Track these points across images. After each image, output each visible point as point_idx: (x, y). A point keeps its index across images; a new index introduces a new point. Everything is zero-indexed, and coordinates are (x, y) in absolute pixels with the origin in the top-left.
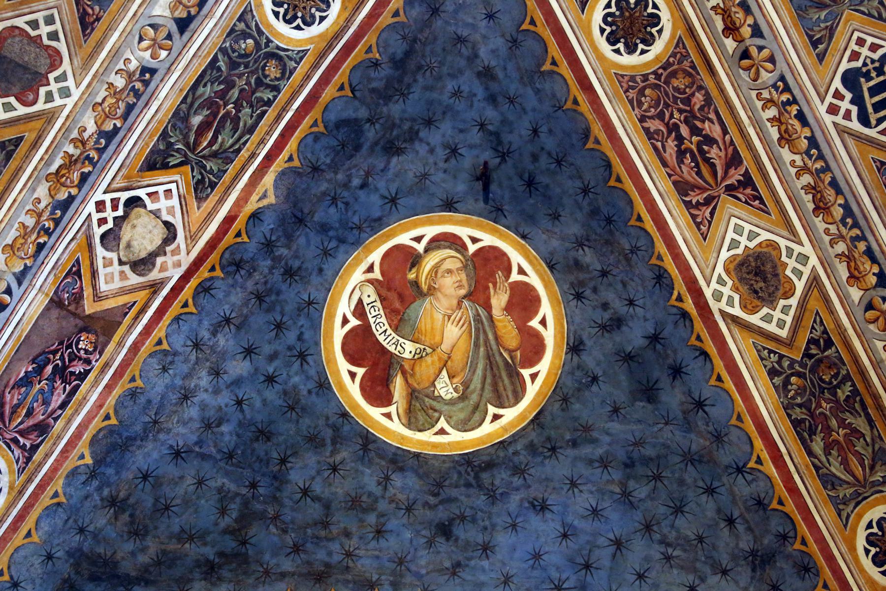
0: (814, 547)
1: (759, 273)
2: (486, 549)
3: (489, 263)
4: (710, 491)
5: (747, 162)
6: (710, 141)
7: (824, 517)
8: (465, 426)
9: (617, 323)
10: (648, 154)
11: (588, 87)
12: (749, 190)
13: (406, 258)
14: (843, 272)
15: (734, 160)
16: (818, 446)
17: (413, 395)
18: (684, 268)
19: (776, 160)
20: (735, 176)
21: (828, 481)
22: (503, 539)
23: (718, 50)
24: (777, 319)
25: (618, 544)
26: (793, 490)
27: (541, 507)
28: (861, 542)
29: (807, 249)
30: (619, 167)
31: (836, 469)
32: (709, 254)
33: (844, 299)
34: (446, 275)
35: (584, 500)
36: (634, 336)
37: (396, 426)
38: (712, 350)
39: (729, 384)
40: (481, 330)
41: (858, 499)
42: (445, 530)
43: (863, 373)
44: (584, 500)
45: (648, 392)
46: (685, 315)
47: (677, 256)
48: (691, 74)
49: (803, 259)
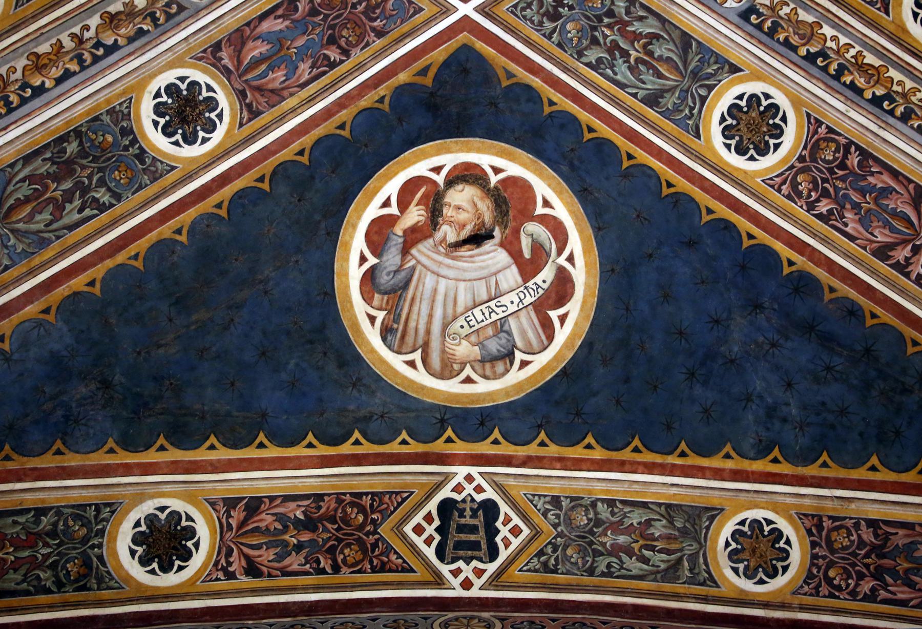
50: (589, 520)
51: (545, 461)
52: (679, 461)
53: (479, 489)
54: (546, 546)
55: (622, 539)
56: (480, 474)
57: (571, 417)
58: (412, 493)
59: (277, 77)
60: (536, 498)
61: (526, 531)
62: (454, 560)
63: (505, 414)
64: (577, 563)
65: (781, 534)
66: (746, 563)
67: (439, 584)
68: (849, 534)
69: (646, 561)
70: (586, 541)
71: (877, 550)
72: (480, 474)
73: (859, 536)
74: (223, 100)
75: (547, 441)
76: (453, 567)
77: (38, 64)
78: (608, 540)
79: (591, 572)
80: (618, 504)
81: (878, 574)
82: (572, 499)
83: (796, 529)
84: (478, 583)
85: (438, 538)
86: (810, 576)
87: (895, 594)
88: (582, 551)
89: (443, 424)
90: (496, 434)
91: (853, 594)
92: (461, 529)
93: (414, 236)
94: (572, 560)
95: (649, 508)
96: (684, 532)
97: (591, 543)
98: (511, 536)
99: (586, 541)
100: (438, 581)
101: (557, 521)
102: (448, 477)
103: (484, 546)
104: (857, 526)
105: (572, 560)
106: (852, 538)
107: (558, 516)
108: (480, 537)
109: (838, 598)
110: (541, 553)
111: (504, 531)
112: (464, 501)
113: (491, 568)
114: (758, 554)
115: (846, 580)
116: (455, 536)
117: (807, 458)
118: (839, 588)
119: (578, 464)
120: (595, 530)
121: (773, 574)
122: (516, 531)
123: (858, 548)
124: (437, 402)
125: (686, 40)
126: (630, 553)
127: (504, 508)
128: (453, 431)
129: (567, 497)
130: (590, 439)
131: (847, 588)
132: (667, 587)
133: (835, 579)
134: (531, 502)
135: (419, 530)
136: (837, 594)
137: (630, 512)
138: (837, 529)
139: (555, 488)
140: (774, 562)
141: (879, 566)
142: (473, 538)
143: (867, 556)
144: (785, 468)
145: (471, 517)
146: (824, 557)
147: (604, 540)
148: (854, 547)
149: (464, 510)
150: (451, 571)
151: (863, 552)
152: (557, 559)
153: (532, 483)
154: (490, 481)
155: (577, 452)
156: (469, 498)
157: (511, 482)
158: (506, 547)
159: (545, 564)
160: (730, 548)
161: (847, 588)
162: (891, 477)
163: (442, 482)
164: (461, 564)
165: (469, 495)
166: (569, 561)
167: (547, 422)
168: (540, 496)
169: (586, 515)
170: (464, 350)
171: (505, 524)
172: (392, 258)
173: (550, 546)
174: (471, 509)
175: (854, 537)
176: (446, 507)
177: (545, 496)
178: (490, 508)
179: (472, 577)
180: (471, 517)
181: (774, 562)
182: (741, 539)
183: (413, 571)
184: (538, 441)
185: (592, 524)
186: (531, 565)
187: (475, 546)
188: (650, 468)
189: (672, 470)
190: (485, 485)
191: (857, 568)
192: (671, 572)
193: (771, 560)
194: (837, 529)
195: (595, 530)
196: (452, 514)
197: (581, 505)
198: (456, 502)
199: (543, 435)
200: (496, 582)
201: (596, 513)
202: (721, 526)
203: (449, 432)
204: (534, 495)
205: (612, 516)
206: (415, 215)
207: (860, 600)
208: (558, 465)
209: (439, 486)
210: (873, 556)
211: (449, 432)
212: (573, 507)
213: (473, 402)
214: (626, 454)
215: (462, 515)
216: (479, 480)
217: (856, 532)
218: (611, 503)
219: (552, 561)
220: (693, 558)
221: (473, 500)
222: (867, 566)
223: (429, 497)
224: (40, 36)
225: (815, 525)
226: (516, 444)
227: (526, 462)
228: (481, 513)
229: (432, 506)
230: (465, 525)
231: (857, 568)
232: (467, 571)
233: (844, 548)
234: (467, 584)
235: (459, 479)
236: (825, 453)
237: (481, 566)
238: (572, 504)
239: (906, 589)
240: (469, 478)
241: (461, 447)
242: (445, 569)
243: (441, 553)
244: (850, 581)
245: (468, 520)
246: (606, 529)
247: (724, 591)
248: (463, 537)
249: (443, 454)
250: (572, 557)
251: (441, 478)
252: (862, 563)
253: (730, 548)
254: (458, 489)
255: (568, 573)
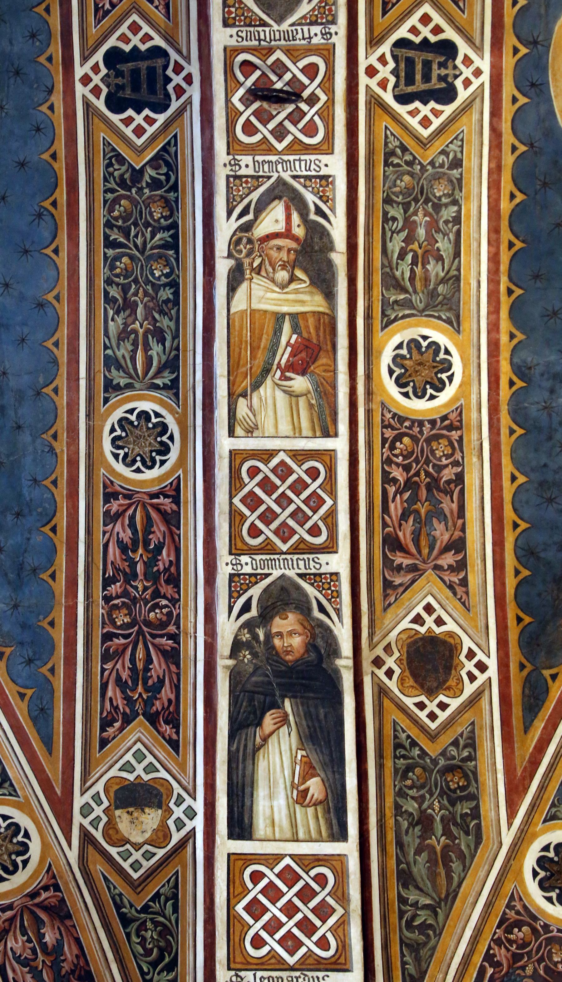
50: (440, 198)
51: (497, 151)
52: (503, 288)
53: (467, 83)
54: (411, 154)
55: (421, 232)
56: (482, 84)
57: (542, 178)
58: (464, 12)
60: (460, 143)
61: (426, 133)
62: (395, 58)
63: (543, 109)
64: (395, 186)
65: (440, 390)
66: (408, 356)
67: (371, 42)
68: (447, 457)
69: (402, 256)
70: (418, 195)
71: (434, 484)
72: (482, 84)
73: (446, 466)
75: (517, 153)
76: (389, 57)
78: (420, 218)
79: (388, 201)
80: (456, 227)
81: (410, 484)
82: (460, 180)
83: (446, 405)
84: (373, 83)
85: (417, 40)
86: (402, 420)
87: (393, 502)
88: (407, 192)
89: (533, 43)
90: (523, 100)
91: (388, 461)
92: (427, 65)
94: (398, 182)
95: (454, 259)
96: (433, 294)
97: (416, 200)
98: (419, 117)
99: (418, 195)
100: (374, 42)
101: (437, 165)
102: (479, 50)
103: (410, 89)
104: (456, 464)
105: (398, 182)
106: (443, 459)
107: (442, 166)
108: (420, 86)
109: (383, 447)
110: (404, 149)
111: (425, 110)
112: (455, 67)
113: (388, 97)
114: (418, 368)
115: (401, 454)
116: (419, 58)
117: (518, 413)
118: (392, 447)
119: (495, 186)
120: (430, 204)
121: (400, 383)
122: (426, 122)
123: (434, 466)
124: (554, 36)
126: (408, 240)
127: (448, 110)
128: (525, 55)
129: (461, 174)
130: (520, 197)
131: (393, 455)
132: (377, 278)
133: (401, 443)
134: (456, 138)
135: (426, 19)
136: (387, 445)
137: (449, 239)
138: (451, 444)
139: (470, 162)
140: (412, 384)
141: (419, 486)
142: (418, 77)
143: (428, 474)
144: (505, 393)
145: (439, 75)
146: (421, 432)
147: (420, 213)
148: (435, 461)
149: (446, 68)
150: (383, 55)
151: (431, 470)
152: (398, 165)
153: (475, 138)
154: (475, 94)
155: (507, 184)
156: (458, 73)
157: (475, 117)
158: (410, 113)
159: (393, 153)
160: (421, 340)
161: (393, 455)
162: (508, 496)
163: (474, 44)
164: (392, 65)
165: (461, 73)
166: (397, 178)
167: (536, 153)
168: (462, 146)
169: (444, 195)
171: (433, 110)
173: (411, 158)
174: (447, 75)
175: (444, 461)
176: (448, 49)
177: (462, 152)
178: (447, 95)
179: (379, 77)
180: (439, 75)
181: (412, 384)
182: (431, 351)
183: (384, 13)
184: (517, 144)
185: (436, 201)
186: (391, 138)
187: (410, 80)
188: (494, 259)
189: (493, 280)
190: (471, 89)
191: (414, 465)
192: (392, 282)
193: (413, 381)
194: (451, 444)
195: (430, 204)
196: (442, 54)
197: (454, 190)
198: (454, 59)
199: (522, 148)
200: (375, 102)
201: (446, 205)
202: (443, 331)
203: (524, 51)
204: (462, 140)
205: (444, 222)
207: (383, 468)
208: (493, 165)
209: (469, 40)
210: (428, 480)
211: (524, 51)
212: (451, 181)
213: (554, 75)
214: (506, 235)
215: (442, 65)
216: (476, 83)
217: (451, 463)
218: (457, 220)
219: (396, 161)
220: (408, 304)
221: (456, 77)
222: (417, 474)
223: (459, 30)
225: (451, 424)
226: (513, 121)
227: (495, 132)
228: (443, 85)
229: (450, 34)
230: (430, 69)
231: (414, 465)
232: (385, 72)
233: (433, 452)
234: (371, 72)
235: (478, 62)
236: (522, 431)
237: (390, 86)
238: (455, 181)
239: (400, 512)
240: (478, 73)
241: (508, 63)
242: (385, 48)
243: (402, 43)
244: (401, 458)
245: (436, 72)
246: (430, 215)
247: (379, 335)
248: (419, 67)
249: (502, 44)
250: (402, 181)
251: (478, 43)
252: (419, 470)
253: (421, 340)
254: (467, 61)
255: (385, 177)
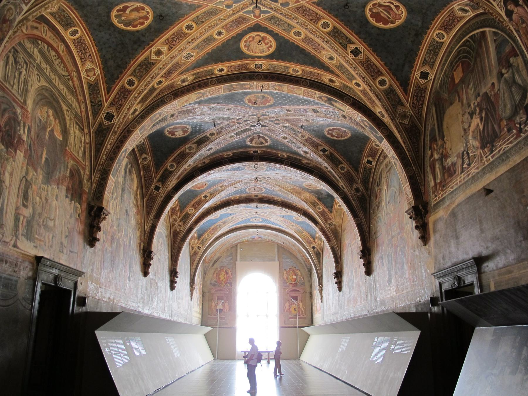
0: (124, 72)
1: (159, 53)
2: (100, 32)
3: (147, 18)
4: (125, 56)
5: (174, 47)
6: (176, 41)
7: (129, 72)
8: (118, 22)
9: (144, 36)
10: (171, 34)
11: (179, 24)
12: (170, 48)
13: (143, 9)
14: (164, 64)
15: (174, 45)
16: (138, 68)
17: (120, 15)
18: (156, 43)
19: (176, 51)
20: (172, 46)
21: (135, 71)
22: (103, 33)
23: (189, 39)
24: (153, 57)
25: (110, 47)
26: (131, 67)
27: (110, 35)
28: (129, 78)
29: (165, 58)
30: (168, 31)
31: (137, 71)
32: (159, 44)
33: (160, 65)
34: (143, 13)
35: (114, 40)
36: (143, 39)
37: (114, 14)
38: (145, 49)
39: (141, 53)
40: (135, 20)
41: (134, 76)
42: (100, 26)
43: (151, 70)
44: (114, 40)
45: (135, 43)
46: (149, 44)
47: (157, 41)
48: (184, 36)
49: (163, 58)
59: (232, 28)
74: (224, 32)
77: (201, 33)
93: (250, 41)
125: (289, 24)
170: (257, 51)
172: (248, 43)
206: (251, 39)
224: (200, 30)
